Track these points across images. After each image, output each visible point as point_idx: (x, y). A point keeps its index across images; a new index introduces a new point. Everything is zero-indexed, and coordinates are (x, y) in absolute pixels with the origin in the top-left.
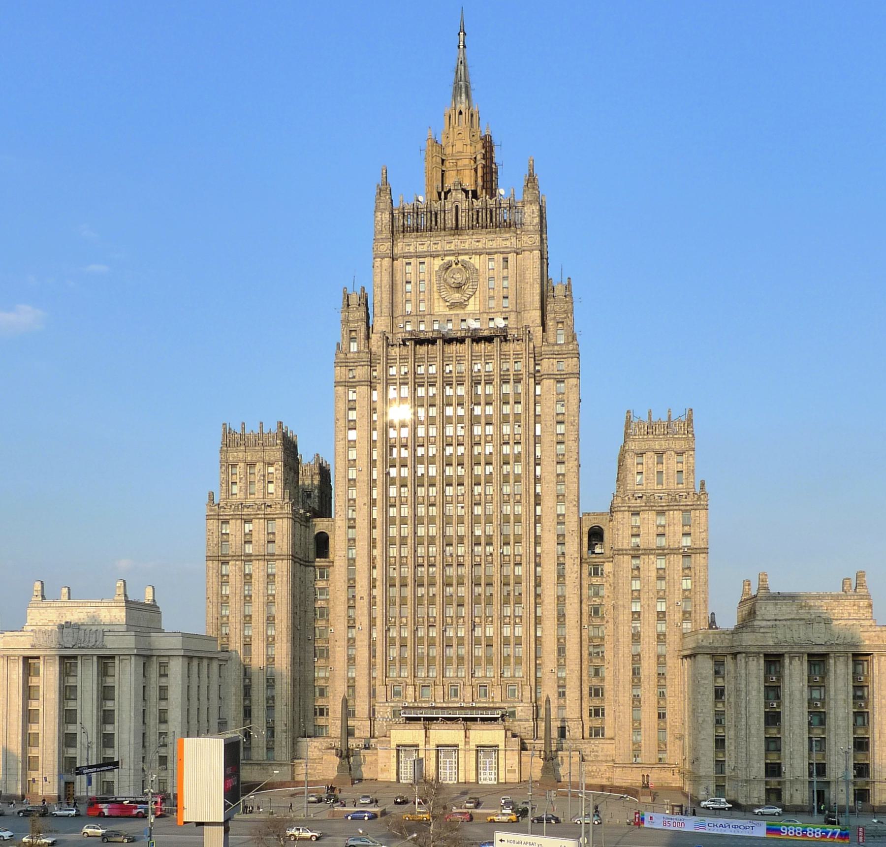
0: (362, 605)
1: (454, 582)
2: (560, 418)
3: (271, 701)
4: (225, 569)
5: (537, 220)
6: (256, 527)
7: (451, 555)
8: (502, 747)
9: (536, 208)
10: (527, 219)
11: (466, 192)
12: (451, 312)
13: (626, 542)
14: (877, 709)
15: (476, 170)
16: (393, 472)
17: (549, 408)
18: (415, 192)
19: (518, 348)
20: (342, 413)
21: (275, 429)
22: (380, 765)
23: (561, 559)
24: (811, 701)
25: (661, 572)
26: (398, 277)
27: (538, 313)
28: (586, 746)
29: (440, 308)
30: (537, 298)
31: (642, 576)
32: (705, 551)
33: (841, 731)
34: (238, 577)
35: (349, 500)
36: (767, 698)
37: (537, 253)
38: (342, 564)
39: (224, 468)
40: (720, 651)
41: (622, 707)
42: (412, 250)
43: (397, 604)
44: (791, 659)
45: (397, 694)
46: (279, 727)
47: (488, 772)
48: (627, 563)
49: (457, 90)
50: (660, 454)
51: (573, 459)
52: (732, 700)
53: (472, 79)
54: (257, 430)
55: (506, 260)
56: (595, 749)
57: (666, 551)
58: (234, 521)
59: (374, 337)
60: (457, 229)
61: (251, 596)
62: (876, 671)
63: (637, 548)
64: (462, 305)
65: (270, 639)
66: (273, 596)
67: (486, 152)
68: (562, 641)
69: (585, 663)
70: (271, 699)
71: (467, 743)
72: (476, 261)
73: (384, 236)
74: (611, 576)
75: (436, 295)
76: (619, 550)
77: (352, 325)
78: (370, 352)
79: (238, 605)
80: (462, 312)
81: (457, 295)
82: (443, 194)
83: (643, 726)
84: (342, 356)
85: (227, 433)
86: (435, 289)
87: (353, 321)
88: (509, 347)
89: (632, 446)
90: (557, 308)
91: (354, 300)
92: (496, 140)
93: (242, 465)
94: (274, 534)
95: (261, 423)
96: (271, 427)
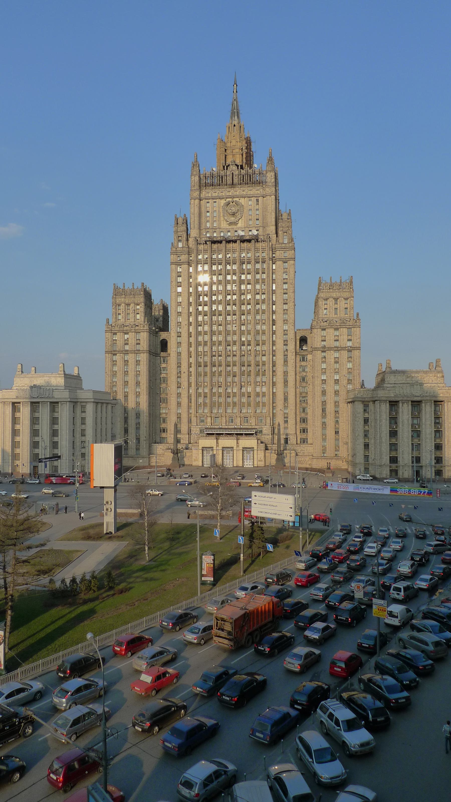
0: (184, 376)
1: (231, 364)
2: (285, 281)
3: (138, 425)
4: (115, 358)
5: (273, 180)
6: (130, 336)
7: (230, 351)
8: (255, 448)
9: (273, 174)
10: (268, 180)
11: (238, 166)
12: (230, 227)
13: (318, 344)
14: (446, 429)
15: (242, 155)
16: (200, 308)
17: (280, 276)
18: (211, 166)
19: (264, 245)
20: (174, 278)
21: (140, 287)
22: (194, 458)
23: (286, 353)
24: (413, 425)
25: (336, 359)
26: (203, 209)
27: (274, 228)
28: (298, 448)
29: (224, 225)
30: (274, 220)
31: (327, 361)
32: (359, 348)
33: (428, 440)
34: (121, 362)
35: (178, 323)
36: (390, 423)
37: (273, 197)
38: (174, 355)
39: (114, 306)
40: (366, 400)
41: (316, 428)
42: (210, 195)
43: (202, 375)
44: (403, 403)
45: (202, 421)
46: (142, 438)
47: (248, 461)
48: (319, 355)
49: (233, 114)
50: (336, 299)
51: (292, 302)
52: (373, 424)
53: (240, 108)
54: (131, 287)
55: (257, 201)
56: (303, 449)
57: (339, 349)
58: (119, 333)
59: (191, 240)
60: (233, 185)
61: (128, 372)
62: (446, 410)
63: (324, 347)
64: (235, 223)
65: (138, 393)
66: (139, 371)
67: (247, 145)
68: (286, 394)
69: (298, 406)
70: (138, 424)
71: (238, 446)
72: (242, 201)
73: (195, 189)
74: (311, 361)
75: (222, 218)
76: (315, 348)
77: (180, 234)
78: (189, 247)
79: (121, 376)
80: (236, 227)
81: (233, 218)
82: (225, 167)
83: (327, 438)
84: (174, 249)
85: (116, 288)
86: (221, 215)
87: (180, 232)
88: (259, 245)
89: (322, 295)
90: (284, 225)
91: (180, 221)
92: (252, 139)
93: (123, 305)
94: (139, 340)
95: (133, 283)
96: (138, 285)
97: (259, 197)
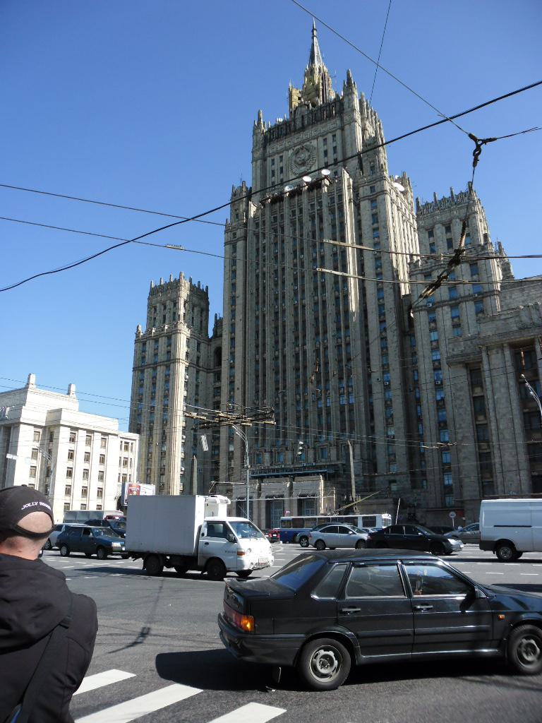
25: (456, 320)
28: (409, 495)
60: (303, 128)
72: (314, 143)
97: (336, 130)
